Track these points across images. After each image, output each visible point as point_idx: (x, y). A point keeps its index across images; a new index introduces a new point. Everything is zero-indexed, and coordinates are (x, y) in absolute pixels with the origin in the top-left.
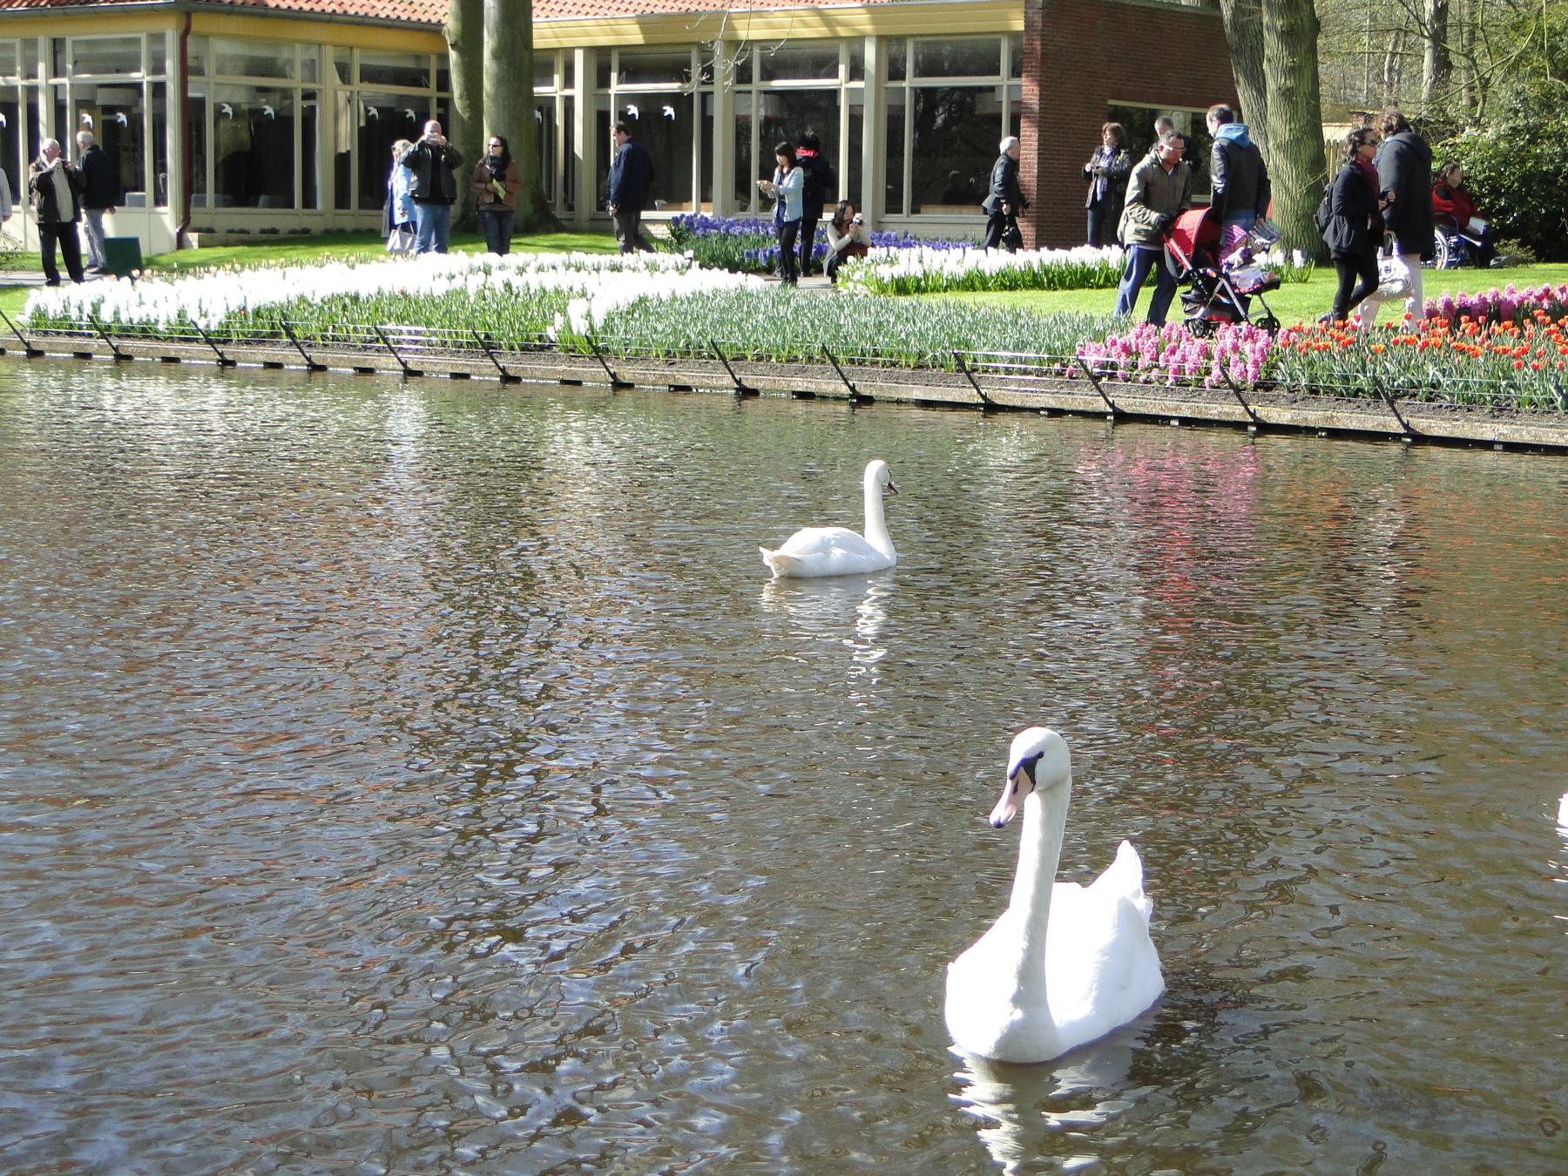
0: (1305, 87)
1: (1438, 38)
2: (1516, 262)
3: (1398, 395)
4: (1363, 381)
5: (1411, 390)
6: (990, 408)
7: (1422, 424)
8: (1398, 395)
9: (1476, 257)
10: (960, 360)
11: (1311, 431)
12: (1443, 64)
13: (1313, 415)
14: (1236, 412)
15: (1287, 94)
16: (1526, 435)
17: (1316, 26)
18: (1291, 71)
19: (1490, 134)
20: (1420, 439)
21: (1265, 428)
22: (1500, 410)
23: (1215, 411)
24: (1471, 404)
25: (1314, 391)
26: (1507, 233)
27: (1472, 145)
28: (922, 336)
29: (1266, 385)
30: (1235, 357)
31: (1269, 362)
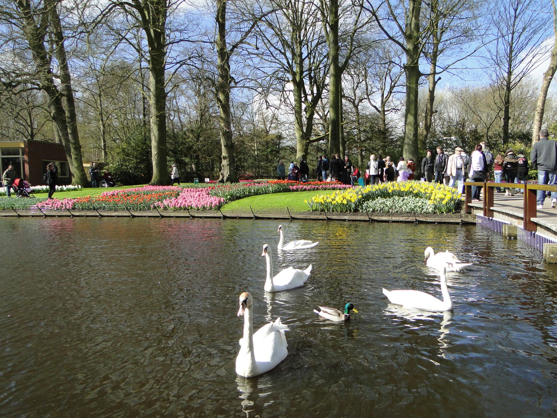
0: (79, 157)
1: (105, 149)
2: (119, 186)
3: (98, 209)
4: (91, 207)
5: (100, 208)
6: (19, 216)
7: (102, 214)
8: (98, 209)
9: (112, 186)
10: (13, 208)
11: (82, 216)
12: (106, 154)
13: (83, 213)
14: (68, 214)
15: (76, 158)
16: (120, 214)
17: (80, 147)
18: (76, 155)
19: (115, 165)
20: (102, 216)
21: (74, 216)
22: (116, 210)
23: (64, 214)
24: (111, 210)
25: (83, 209)
26: (118, 181)
27: (112, 167)
28: (4, 204)
29: (74, 209)
30: (67, 204)
31: (74, 204)
